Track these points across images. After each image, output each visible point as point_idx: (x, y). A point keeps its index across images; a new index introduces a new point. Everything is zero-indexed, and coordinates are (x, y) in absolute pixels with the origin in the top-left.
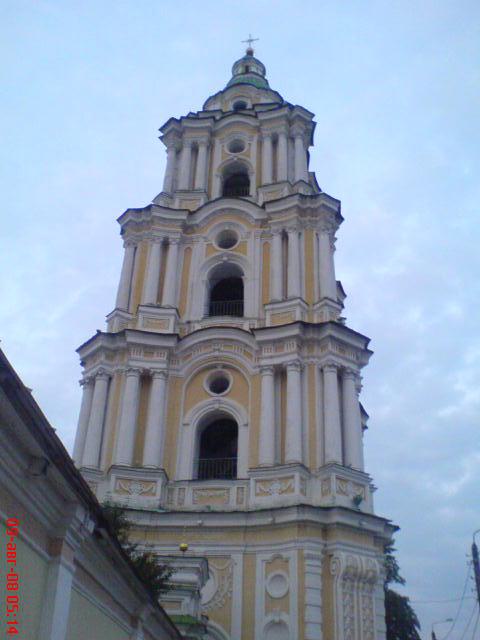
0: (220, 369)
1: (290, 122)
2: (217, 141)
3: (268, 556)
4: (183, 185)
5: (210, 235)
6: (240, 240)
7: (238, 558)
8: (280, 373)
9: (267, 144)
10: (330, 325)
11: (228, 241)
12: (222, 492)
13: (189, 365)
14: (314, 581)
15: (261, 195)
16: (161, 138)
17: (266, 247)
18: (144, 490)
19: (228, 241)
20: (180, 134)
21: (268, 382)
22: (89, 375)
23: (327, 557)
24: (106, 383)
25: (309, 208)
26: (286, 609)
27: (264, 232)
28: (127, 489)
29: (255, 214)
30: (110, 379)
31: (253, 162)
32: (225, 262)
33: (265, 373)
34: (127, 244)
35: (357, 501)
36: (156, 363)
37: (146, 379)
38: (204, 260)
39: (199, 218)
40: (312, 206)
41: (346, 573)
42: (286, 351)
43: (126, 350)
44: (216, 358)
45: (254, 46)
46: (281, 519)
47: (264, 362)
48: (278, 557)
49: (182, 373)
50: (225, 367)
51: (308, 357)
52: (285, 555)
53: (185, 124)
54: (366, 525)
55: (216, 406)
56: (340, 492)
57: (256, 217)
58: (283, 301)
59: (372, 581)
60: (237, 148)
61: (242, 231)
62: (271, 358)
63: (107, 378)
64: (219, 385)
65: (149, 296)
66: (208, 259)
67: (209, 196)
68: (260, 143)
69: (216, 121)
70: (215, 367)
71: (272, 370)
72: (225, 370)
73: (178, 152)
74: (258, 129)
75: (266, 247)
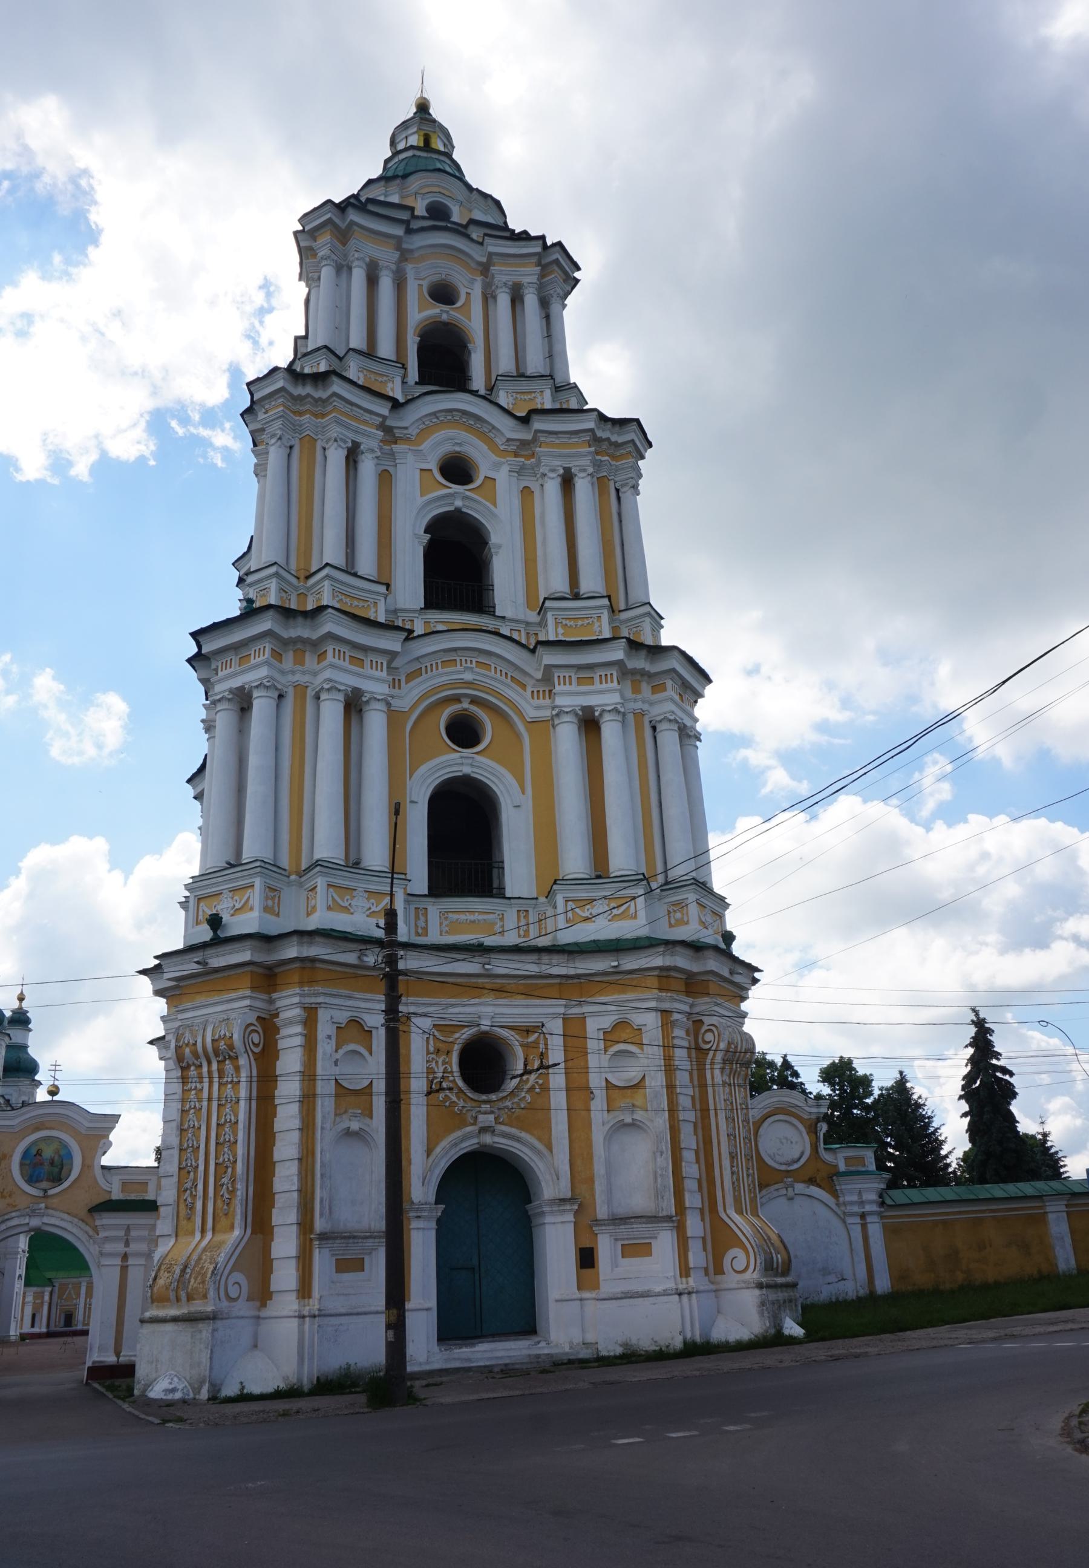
0: (465, 704)
1: (545, 269)
2: (410, 269)
6: (483, 471)
7: (556, 1026)
9: (503, 300)
10: (676, 653)
11: (457, 470)
12: (491, 916)
13: (429, 684)
18: (374, 909)
25: (608, 439)
27: (523, 467)
28: (346, 904)
29: (508, 428)
31: (474, 326)
32: (458, 511)
33: (566, 718)
36: (374, 683)
38: (420, 501)
40: (614, 438)
42: (597, 686)
43: (315, 646)
44: (468, 684)
46: (631, 962)
50: (475, 701)
51: (635, 701)
55: (467, 770)
57: (511, 435)
61: (486, 462)
62: (571, 697)
64: (464, 733)
66: (425, 498)
68: (488, 298)
69: (409, 231)
70: (457, 699)
71: (577, 715)
72: (474, 708)
74: (485, 269)
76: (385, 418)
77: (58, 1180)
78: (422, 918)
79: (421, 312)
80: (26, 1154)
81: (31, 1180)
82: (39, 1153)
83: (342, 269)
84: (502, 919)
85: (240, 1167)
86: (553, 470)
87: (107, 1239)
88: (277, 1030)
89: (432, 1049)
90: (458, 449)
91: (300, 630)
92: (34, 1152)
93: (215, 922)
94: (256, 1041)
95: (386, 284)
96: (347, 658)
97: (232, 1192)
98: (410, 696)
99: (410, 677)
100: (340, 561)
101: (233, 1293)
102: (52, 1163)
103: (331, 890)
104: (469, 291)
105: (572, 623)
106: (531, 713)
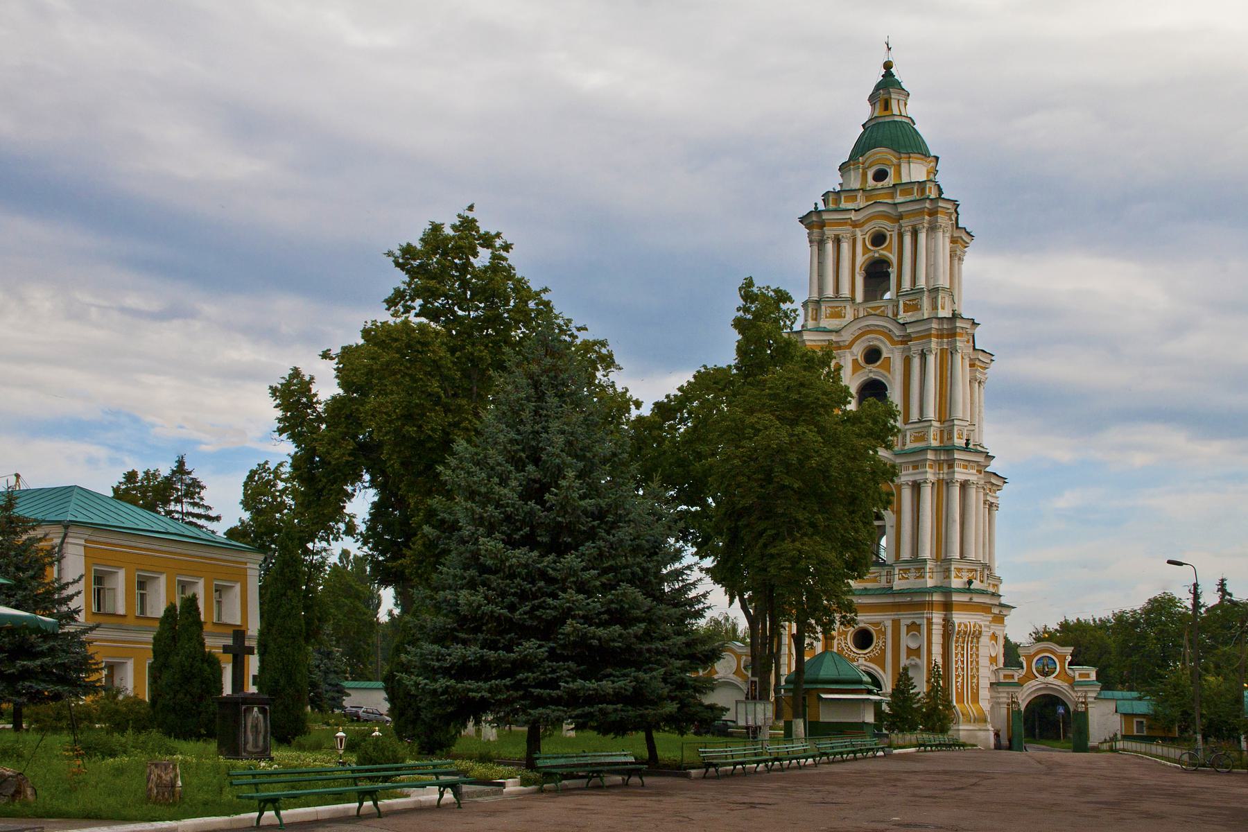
3: (909, 622)
5: (858, 350)
6: (885, 355)
7: (889, 624)
8: (917, 487)
14: (937, 639)
15: (901, 303)
19: (873, 355)
20: (822, 225)
21: (907, 494)
23: (947, 624)
26: (919, 657)
31: (893, 258)
35: (970, 582)
41: (959, 632)
45: (894, 57)
48: (914, 623)
52: (918, 622)
54: (976, 599)
56: (957, 577)
58: (920, 421)
59: (977, 635)
60: (878, 239)
67: (853, 299)
73: (821, 243)
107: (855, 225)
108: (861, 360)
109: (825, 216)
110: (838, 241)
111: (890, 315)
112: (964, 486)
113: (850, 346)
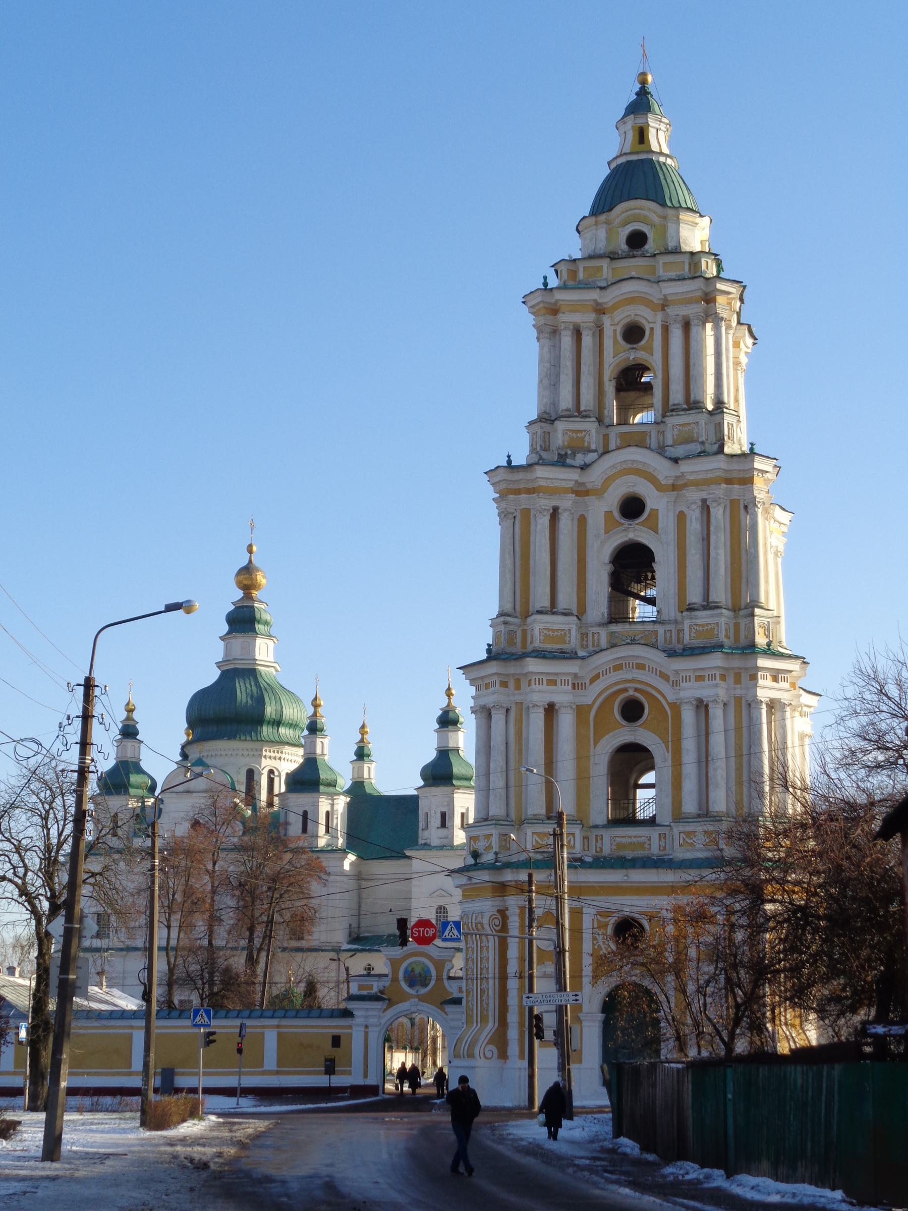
0: (631, 693)
4: (566, 401)
5: (612, 500)
6: (650, 505)
9: (676, 335)
11: (632, 507)
16: (524, 302)
17: (681, 518)
19: (632, 507)
22: (483, 701)
24: (503, 717)
30: (507, 710)
31: (656, 360)
34: (503, 515)
36: (562, 696)
37: (551, 710)
39: (595, 477)
44: (632, 681)
47: (684, 694)
49: (588, 700)
53: (560, 296)
60: (633, 333)
63: (504, 711)
64: (632, 711)
65: (541, 598)
68: (666, 329)
75: (681, 518)
76: (576, 481)
77: (426, 985)
78: (600, 841)
79: (616, 355)
80: (406, 970)
81: (411, 985)
82: (413, 970)
83: (555, 332)
84: (649, 840)
85: (491, 992)
86: (695, 503)
87: (452, 1020)
88: (508, 918)
89: (596, 926)
90: (631, 490)
91: (512, 669)
92: (410, 969)
93: (475, 855)
94: (497, 923)
95: (587, 340)
96: (545, 682)
97: (488, 1004)
98: (591, 695)
99: (592, 681)
100: (547, 603)
101: (489, 1055)
102: (420, 976)
103: (535, 836)
104: (651, 325)
105: (701, 629)
106: (671, 698)
107: (600, 310)
108: (617, 514)
109: (560, 296)
110: (578, 333)
111: (654, 445)
112: (772, 705)
113: (599, 492)
